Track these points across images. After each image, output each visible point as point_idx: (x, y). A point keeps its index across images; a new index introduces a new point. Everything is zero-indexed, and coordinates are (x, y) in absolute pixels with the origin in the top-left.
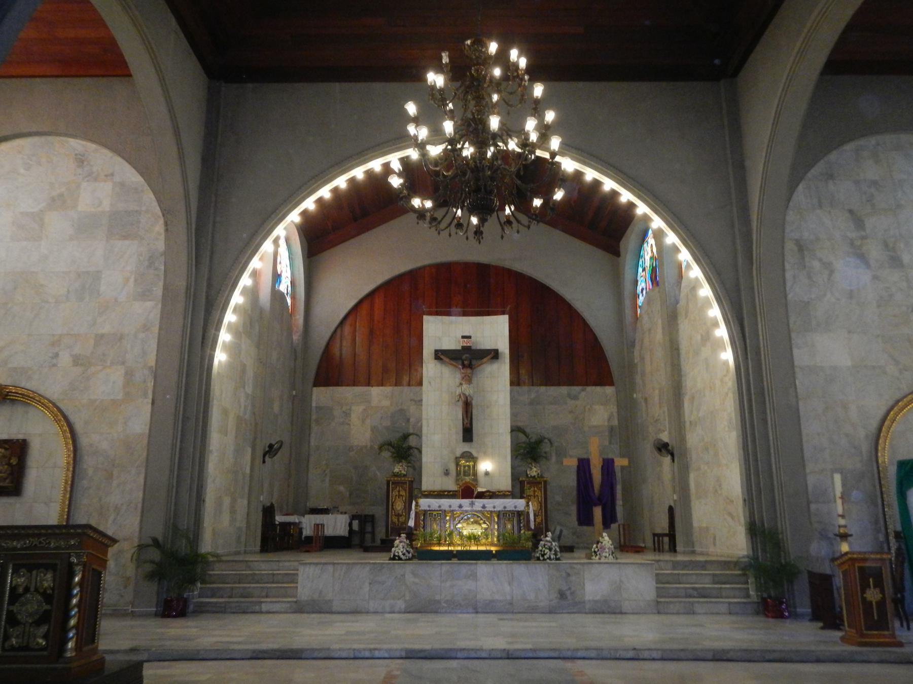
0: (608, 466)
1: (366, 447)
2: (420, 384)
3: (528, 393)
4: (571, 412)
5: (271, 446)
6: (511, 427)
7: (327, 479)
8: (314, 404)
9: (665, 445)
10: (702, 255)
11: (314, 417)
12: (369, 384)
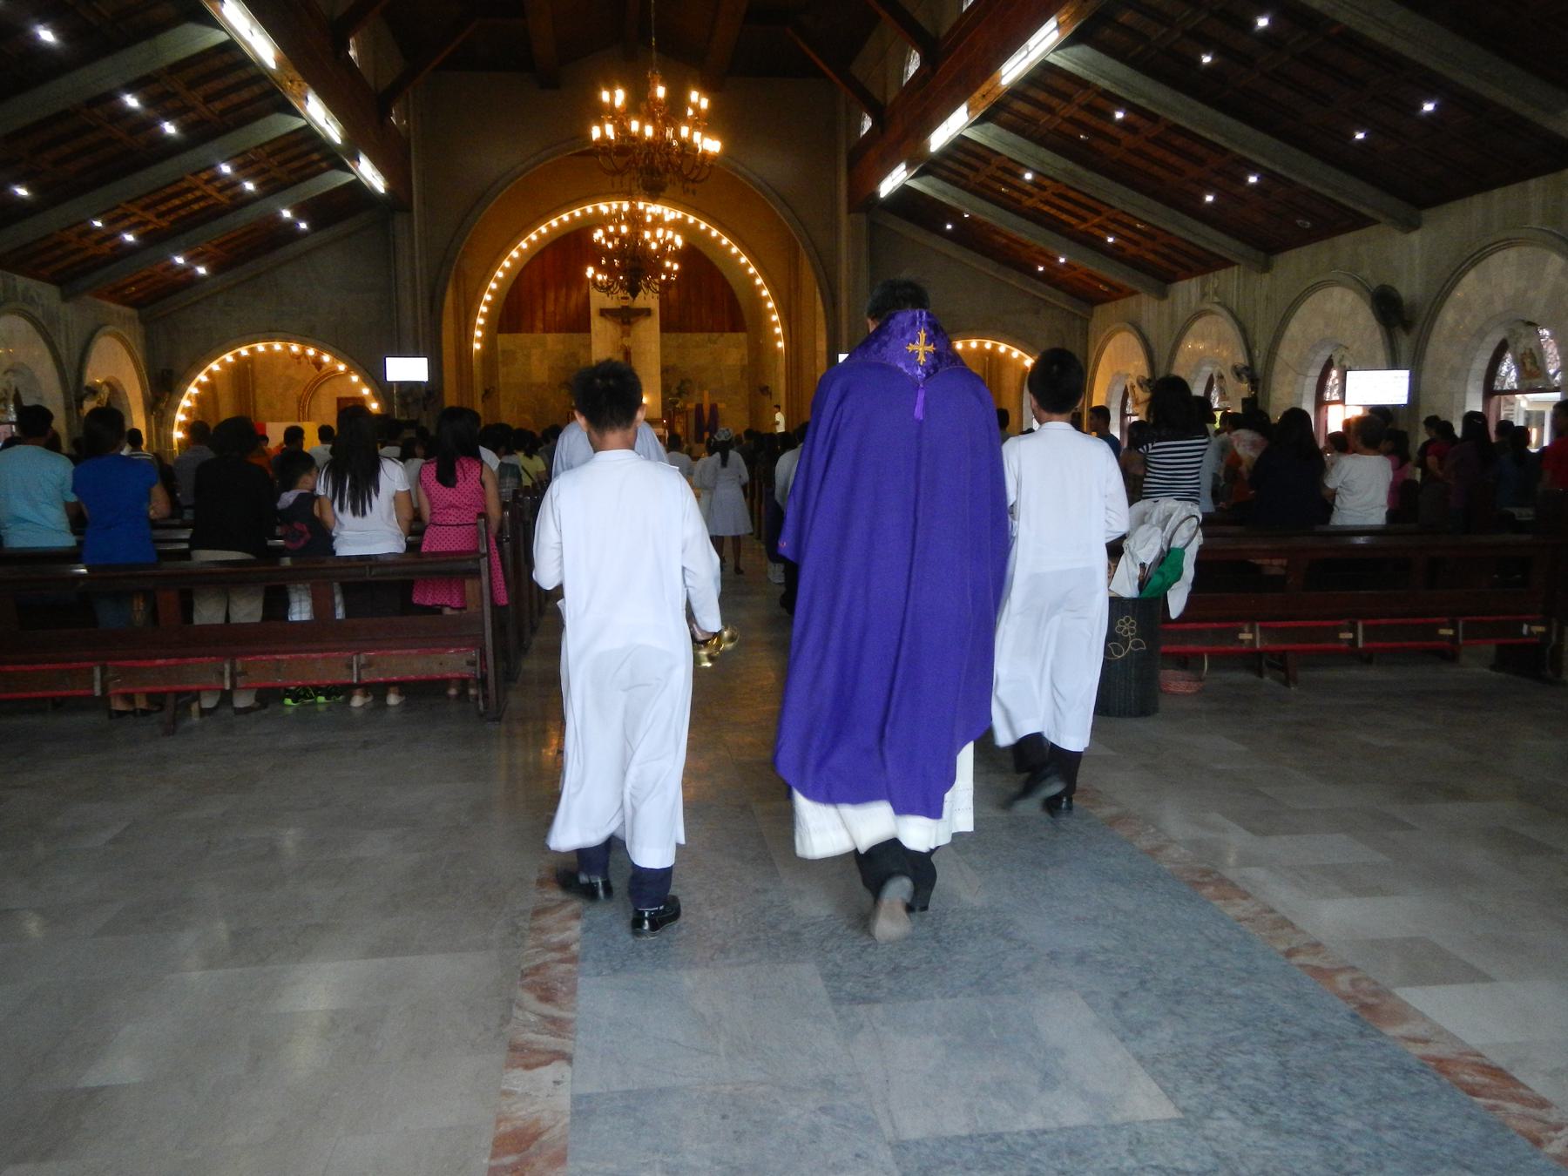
0: (714, 408)
1: (544, 384)
2: (588, 330)
3: (675, 338)
4: (711, 354)
5: (487, 392)
6: (662, 367)
7: (516, 409)
8: (499, 348)
9: (767, 388)
10: (770, 282)
11: (500, 358)
12: (546, 330)
